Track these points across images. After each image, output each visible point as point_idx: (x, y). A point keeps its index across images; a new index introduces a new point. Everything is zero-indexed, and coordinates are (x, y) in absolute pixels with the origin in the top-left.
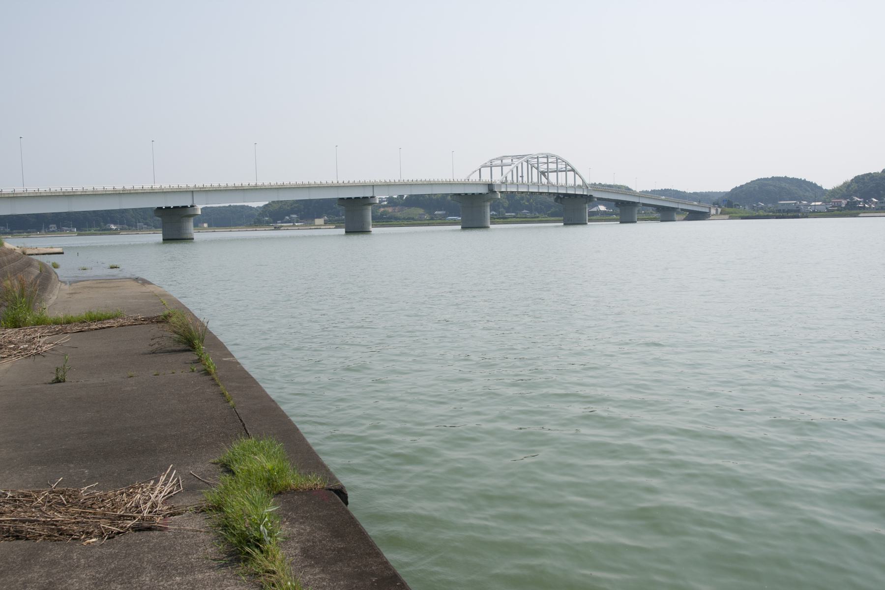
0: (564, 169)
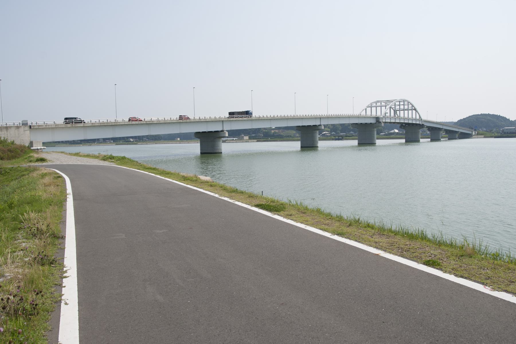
0: (399, 109)
